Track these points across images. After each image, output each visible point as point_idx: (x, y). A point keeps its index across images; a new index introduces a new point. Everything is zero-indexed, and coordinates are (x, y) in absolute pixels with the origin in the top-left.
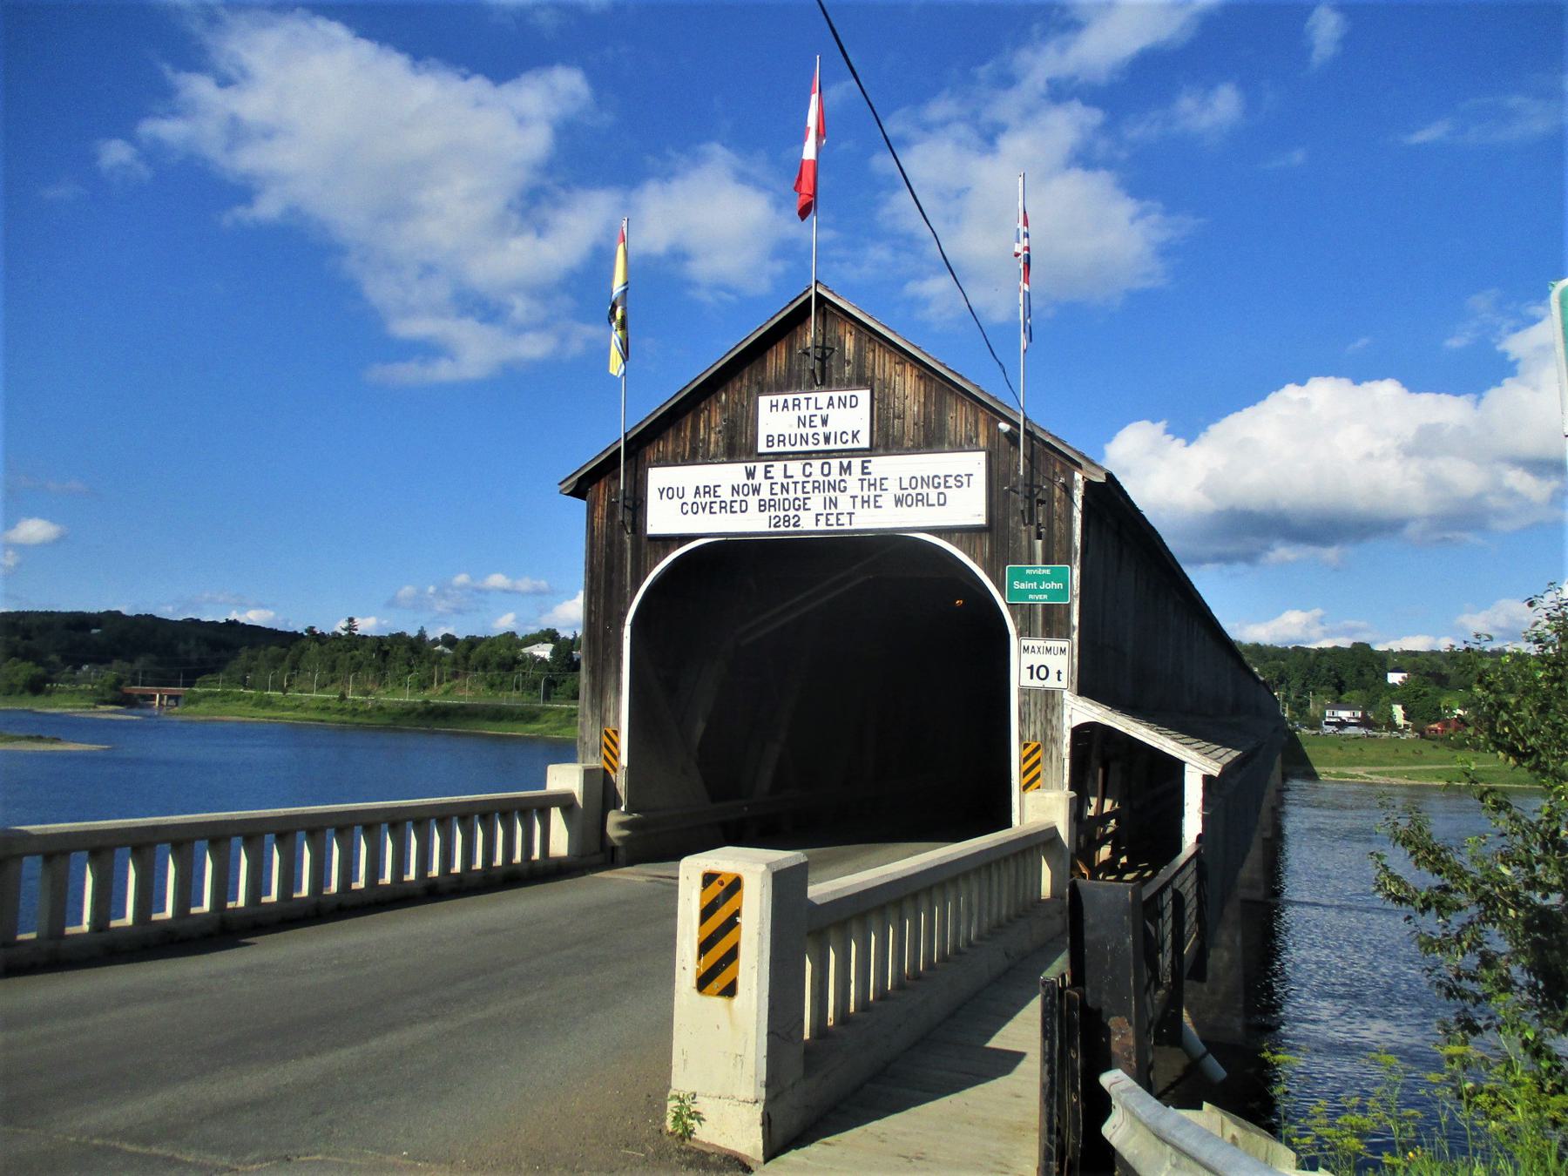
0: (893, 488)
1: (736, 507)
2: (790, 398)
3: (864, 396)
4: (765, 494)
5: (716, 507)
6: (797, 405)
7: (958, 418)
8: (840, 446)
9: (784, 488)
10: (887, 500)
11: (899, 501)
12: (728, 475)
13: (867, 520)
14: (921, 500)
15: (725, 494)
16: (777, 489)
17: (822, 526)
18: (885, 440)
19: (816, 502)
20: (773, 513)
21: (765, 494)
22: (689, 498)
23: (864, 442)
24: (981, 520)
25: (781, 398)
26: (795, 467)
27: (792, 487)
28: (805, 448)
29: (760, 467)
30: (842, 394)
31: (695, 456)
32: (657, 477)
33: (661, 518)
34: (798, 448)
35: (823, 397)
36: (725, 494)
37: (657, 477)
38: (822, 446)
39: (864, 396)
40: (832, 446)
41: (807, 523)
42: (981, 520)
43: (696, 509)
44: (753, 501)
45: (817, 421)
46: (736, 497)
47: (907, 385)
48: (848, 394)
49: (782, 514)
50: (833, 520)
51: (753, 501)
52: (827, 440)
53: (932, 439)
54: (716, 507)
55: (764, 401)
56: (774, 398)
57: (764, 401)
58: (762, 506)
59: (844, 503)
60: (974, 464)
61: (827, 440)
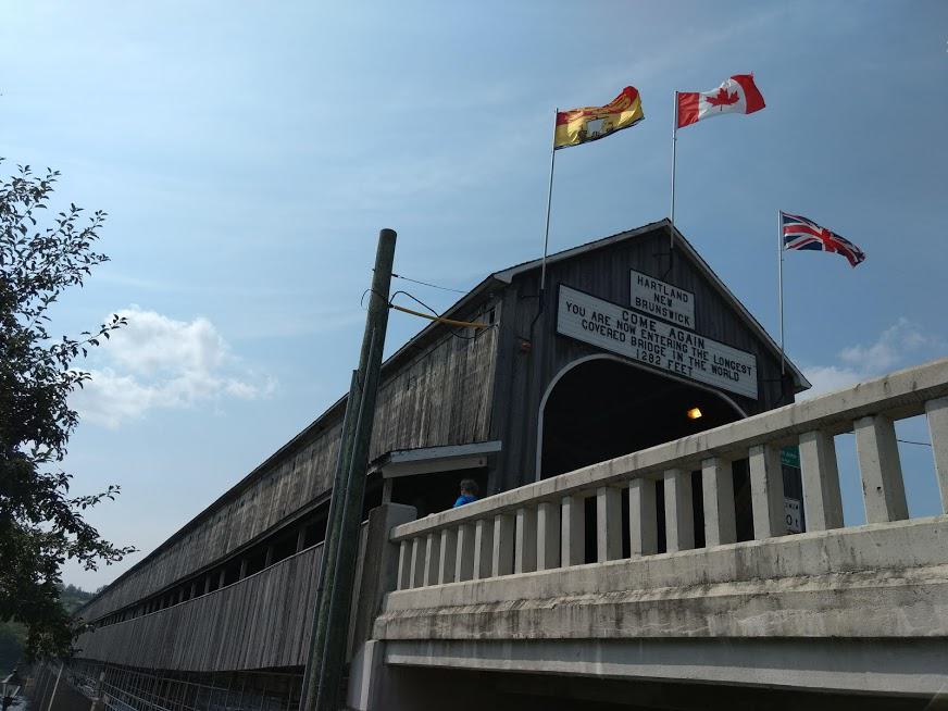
1: (618, 335)
2: (650, 280)
3: (691, 297)
4: (638, 335)
5: (605, 331)
6: (654, 286)
8: (678, 322)
9: (650, 336)
10: (708, 366)
11: (714, 369)
12: (614, 313)
13: (697, 374)
14: (726, 374)
15: (614, 326)
16: (646, 335)
17: (672, 368)
18: (702, 329)
19: (669, 352)
20: (641, 350)
21: (638, 335)
22: (588, 317)
23: (692, 326)
25: (645, 277)
27: (655, 338)
28: (658, 315)
30: (680, 291)
32: (567, 295)
33: (569, 325)
34: (654, 313)
35: (669, 288)
36: (614, 326)
37: (567, 295)
38: (668, 318)
40: (673, 320)
41: (664, 364)
43: (591, 327)
44: (628, 335)
45: (665, 301)
46: (619, 330)
48: (683, 292)
49: (648, 353)
50: (679, 368)
52: (671, 317)
54: (605, 331)
56: (641, 275)
61: (671, 317)
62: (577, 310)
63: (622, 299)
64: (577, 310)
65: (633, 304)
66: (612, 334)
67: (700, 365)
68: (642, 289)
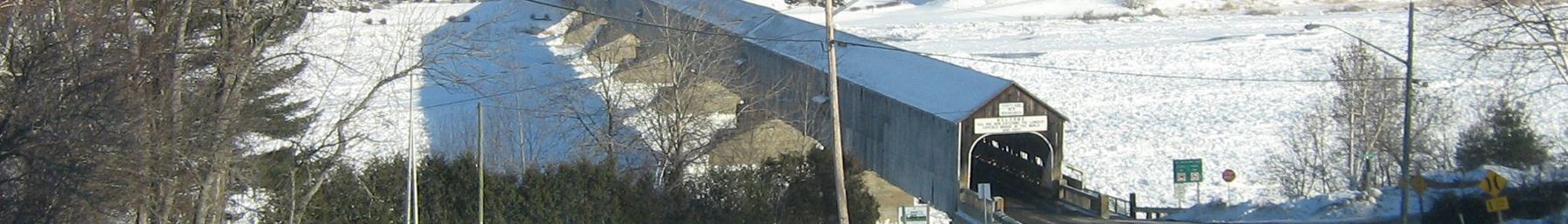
0: (1028, 123)
3: (1022, 104)
7: (1041, 109)
10: (1028, 126)
12: (994, 120)
18: (1027, 113)
19: (1013, 126)
22: (985, 125)
23: (1022, 114)
24: (1046, 129)
26: (1008, 119)
29: (1000, 119)
31: (984, 116)
32: (977, 121)
37: (977, 121)
39: (1022, 104)
42: (1046, 129)
43: (987, 128)
44: (999, 126)
47: (1031, 103)
51: (999, 126)
53: (1036, 113)
55: (1001, 105)
57: (1001, 105)
58: (1002, 127)
59: (1019, 126)
60: (1045, 118)
62: (979, 124)
63: (995, 114)
64: (979, 124)
65: (1000, 114)
66: (993, 127)
67: (1024, 126)
68: (1004, 108)
